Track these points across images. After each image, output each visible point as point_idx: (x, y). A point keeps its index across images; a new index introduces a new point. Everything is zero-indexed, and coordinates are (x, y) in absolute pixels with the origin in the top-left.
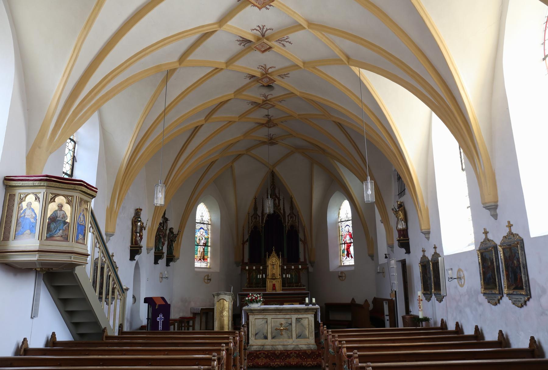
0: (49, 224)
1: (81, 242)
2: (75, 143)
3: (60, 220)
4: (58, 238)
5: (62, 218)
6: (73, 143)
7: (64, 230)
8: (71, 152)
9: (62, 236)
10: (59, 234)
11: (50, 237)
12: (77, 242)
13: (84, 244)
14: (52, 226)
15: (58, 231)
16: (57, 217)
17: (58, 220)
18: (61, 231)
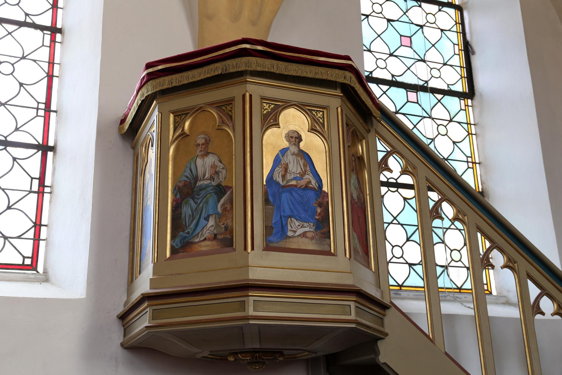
0: (176, 208)
1: (311, 246)
2: (459, 8)
3: (207, 186)
4: (205, 246)
5: (212, 178)
6: (452, 11)
7: (219, 217)
8: (454, 37)
9: (215, 237)
10: (207, 233)
11: (183, 246)
12: (268, 248)
13: (329, 253)
14: (186, 211)
15: (203, 222)
16: (196, 179)
17: (201, 189)
18: (211, 222)
